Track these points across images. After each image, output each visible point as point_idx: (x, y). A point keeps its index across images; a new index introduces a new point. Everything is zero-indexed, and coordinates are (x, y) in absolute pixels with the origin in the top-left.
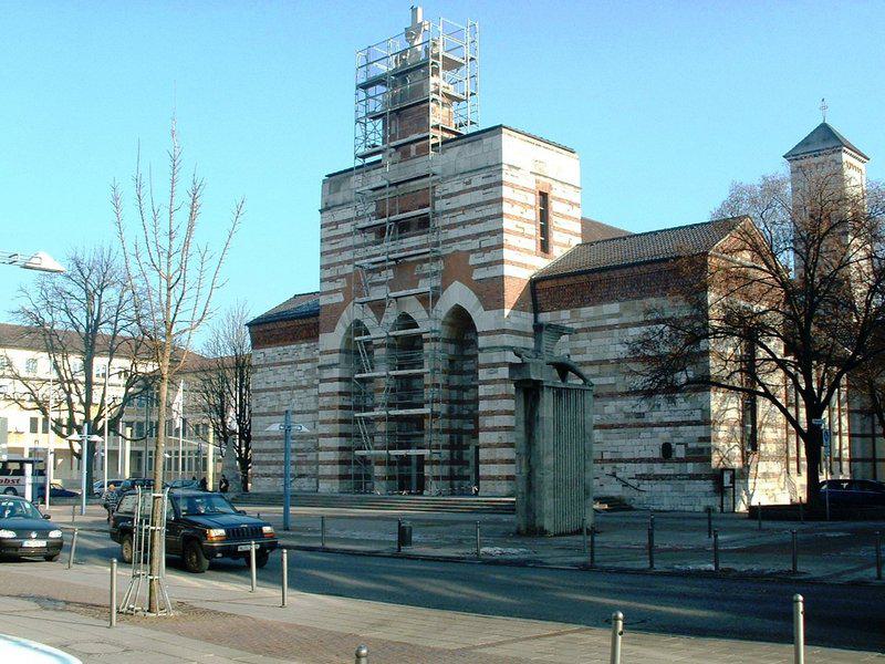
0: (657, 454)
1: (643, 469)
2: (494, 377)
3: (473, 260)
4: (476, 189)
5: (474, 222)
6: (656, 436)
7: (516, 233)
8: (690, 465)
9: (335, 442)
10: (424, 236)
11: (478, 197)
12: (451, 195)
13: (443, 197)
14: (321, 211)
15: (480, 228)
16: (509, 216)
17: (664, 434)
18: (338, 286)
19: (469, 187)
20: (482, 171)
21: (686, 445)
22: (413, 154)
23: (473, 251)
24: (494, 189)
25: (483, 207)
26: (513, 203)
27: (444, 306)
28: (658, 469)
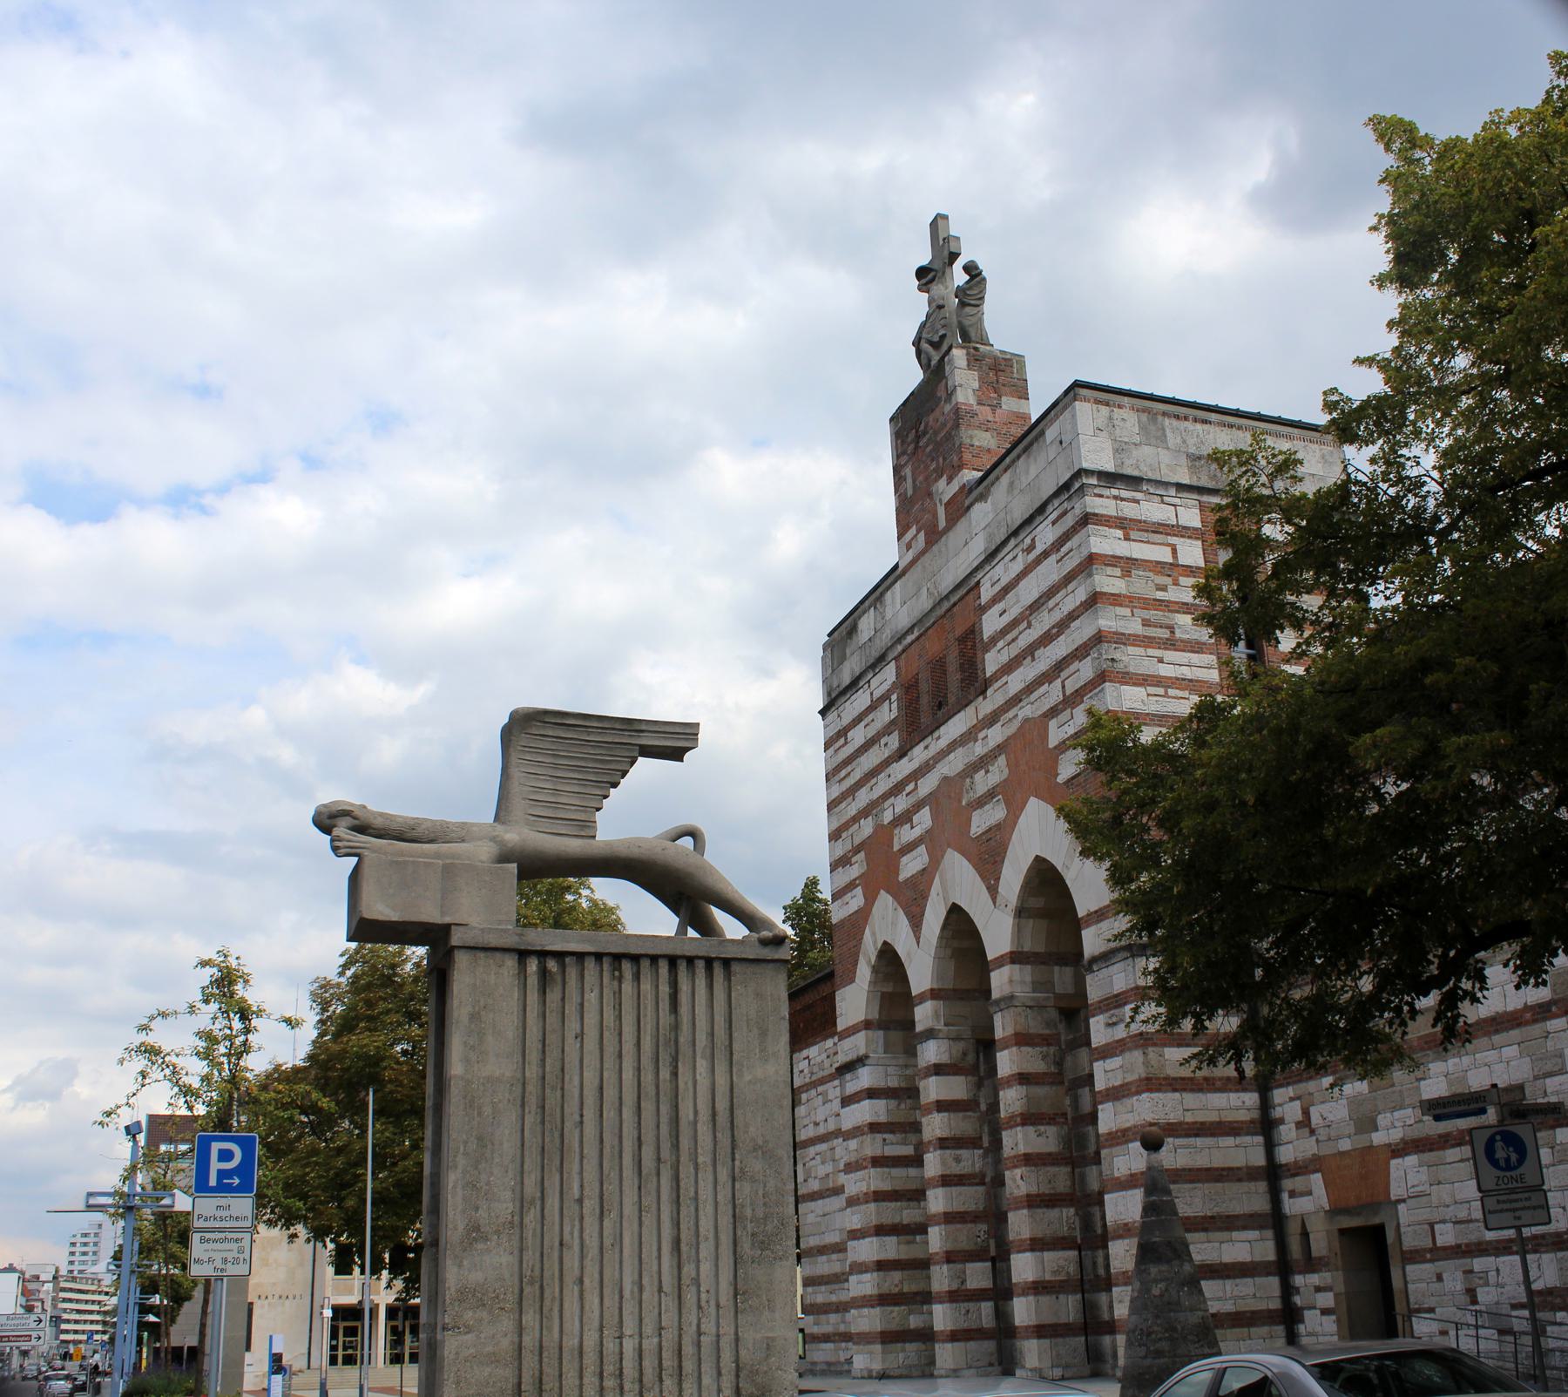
4: (1045, 554)
5: (1047, 639)
7: (1147, 642)
9: (867, 1250)
10: (970, 710)
11: (1050, 572)
12: (1006, 590)
13: (995, 600)
14: (823, 712)
15: (1060, 649)
16: (1116, 600)
18: (854, 871)
19: (1032, 556)
22: (942, 523)
23: (1053, 712)
26: (1128, 565)
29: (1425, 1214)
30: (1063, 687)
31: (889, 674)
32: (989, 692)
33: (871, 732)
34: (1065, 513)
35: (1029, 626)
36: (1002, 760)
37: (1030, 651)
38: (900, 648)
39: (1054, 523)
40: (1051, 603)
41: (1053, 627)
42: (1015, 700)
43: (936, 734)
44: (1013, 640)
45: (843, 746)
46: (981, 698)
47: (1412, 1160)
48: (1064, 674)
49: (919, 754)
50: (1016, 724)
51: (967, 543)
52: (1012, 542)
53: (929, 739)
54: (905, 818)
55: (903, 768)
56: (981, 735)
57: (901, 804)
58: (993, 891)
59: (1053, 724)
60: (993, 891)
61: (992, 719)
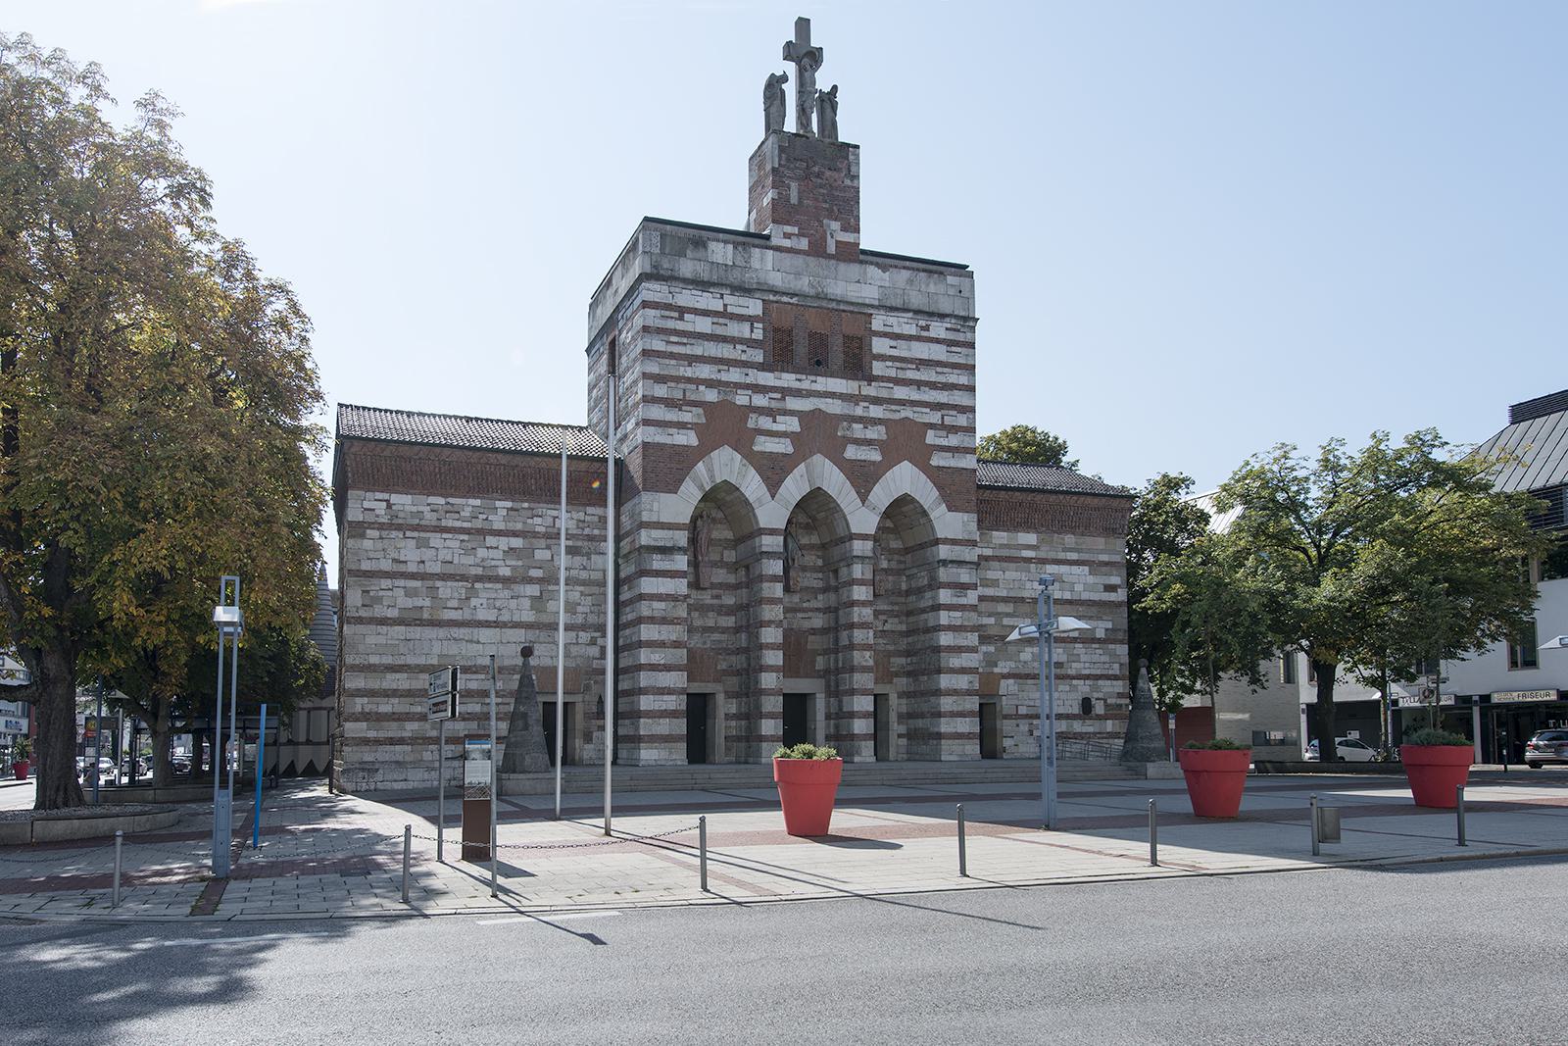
0: (1076, 710)
1: (1062, 726)
2: (963, 601)
3: (931, 438)
4: (937, 341)
5: (933, 386)
6: (1074, 688)
8: (1109, 722)
11: (939, 352)
17: (1083, 688)
18: (686, 417)
20: (948, 320)
21: (1105, 701)
23: (932, 426)
24: (964, 350)
25: (945, 370)
27: (883, 494)
28: (1078, 726)
29: (1017, 702)
30: (943, 418)
31: (754, 307)
32: (873, 384)
33: (720, 331)
34: (959, 331)
35: (919, 370)
36: (882, 429)
37: (919, 384)
40: (939, 369)
42: (902, 403)
43: (813, 378)
44: (902, 369)
45: (676, 319)
46: (866, 383)
47: (1011, 681)
48: (944, 412)
49: (788, 380)
50: (897, 416)
51: (858, 282)
52: (910, 315)
53: (804, 377)
55: (767, 379)
56: (863, 404)
57: (760, 401)
58: (864, 497)
59: (930, 433)
60: (864, 498)
61: (876, 401)
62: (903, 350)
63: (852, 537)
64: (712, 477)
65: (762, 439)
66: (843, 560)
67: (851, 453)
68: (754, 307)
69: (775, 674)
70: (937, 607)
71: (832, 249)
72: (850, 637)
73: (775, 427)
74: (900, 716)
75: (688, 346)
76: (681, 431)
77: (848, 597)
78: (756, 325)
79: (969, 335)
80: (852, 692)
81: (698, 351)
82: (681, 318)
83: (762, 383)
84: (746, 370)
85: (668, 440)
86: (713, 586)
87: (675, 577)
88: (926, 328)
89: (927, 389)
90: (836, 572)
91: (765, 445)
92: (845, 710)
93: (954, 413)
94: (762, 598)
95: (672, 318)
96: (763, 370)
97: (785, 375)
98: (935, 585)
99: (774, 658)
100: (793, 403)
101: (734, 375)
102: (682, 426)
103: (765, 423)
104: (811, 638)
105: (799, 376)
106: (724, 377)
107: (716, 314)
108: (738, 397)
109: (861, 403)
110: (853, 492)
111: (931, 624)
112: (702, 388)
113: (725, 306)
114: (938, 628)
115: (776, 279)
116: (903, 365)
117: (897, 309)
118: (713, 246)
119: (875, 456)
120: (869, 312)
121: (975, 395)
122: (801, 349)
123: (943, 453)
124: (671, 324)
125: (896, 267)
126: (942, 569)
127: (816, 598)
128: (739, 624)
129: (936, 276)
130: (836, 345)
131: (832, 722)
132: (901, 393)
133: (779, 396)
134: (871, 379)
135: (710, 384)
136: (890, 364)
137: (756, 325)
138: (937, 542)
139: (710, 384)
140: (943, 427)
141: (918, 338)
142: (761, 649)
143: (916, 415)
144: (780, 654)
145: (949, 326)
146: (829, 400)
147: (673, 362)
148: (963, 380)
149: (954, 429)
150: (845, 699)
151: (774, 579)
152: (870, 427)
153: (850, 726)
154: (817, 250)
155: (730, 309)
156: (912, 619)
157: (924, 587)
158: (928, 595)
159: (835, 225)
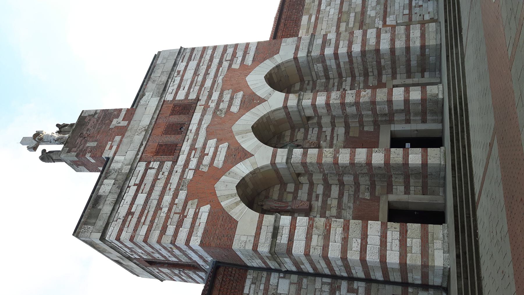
2: (333, 41)
3: (236, 66)
4: (186, 66)
5: (209, 67)
10: (198, 107)
11: (193, 64)
15: (216, 61)
18: (191, 212)
23: (230, 65)
24: (195, 53)
25: (202, 61)
30: (227, 61)
31: (142, 166)
32: (200, 98)
34: (184, 56)
35: (199, 74)
36: (226, 92)
37: (207, 73)
38: (140, 154)
39: (182, 62)
40: (201, 64)
41: (208, 64)
43: (189, 131)
44: (196, 83)
45: (132, 217)
46: (199, 102)
48: (224, 60)
49: (186, 147)
51: (146, 108)
52: (170, 80)
53: (187, 137)
54: (203, 155)
58: (262, 100)
59: (234, 66)
60: (262, 100)
62: (186, 84)
63: (285, 107)
64: (232, 196)
65: (216, 162)
66: (300, 112)
67: (235, 109)
68: (142, 166)
69: (373, 154)
70: (336, 55)
71: (125, 123)
72: (351, 105)
73: (211, 154)
74: (409, 77)
75: (150, 210)
76: (199, 217)
77: (323, 108)
78: (151, 166)
79: (188, 51)
80: (390, 102)
81: (155, 202)
82: (133, 214)
83: (183, 162)
84: (174, 172)
85: (203, 226)
86: (309, 199)
87: (295, 227)
88: (179, 72)
89: (210, 70)
90: (309, 118)
91: (219, 162)
92: (403, 108)
93: (225, 55)
94: (317, 163)
95: (131, 220)
96: (177, 161)
97: (183, 149)
98: (322, 58)
99: (361, 154)
100: (199, 145)
101: (175, 179)
102: (196, 215)
103: (207, 160)
104: (351, 134)
105: (186, 140)
106: (174, 186)
107: (137, 191)
108: (188, 178)
109: (209, 105)
110: (258, 107)
111: (347, 60)
112: (176, 201)
113: (135, 185)
114: (350, 54)
115: (131, 155)
116: (195, 82)
117: (165, 87)
118: (101, 192)
119: (240, 94)
120: (162, 102)
121: (219, 46)
122: (171, 139)
123: (246, 59)
124: (134, 220)
125: (145, 89)
126: (312, 54)
127: (325, 132)
128: (337, 182)
129: (155, 69)
130: (176, 119)
131: (411, 118)
132: (208, 83)
133: (194, 152)
134: (198, 99)
135: (175, 195)
136: (192, 90)
137: (151, 166)
138: (296, 58)
139: (175, 195)
140: (231, 61)
141: (183, 76)
142: (354, 164)
143: (222, 74)
144: (358, 150)
145: (181, 61)
146: (203, 123)
147: (156, 221)
148: (210, 52)
149: (234, 55)
150: (395, 107)
151: (305, 154)
152: (223, 99)
153: (415, 103)
154: (122, 131)
155: (137, 182)
156: (344, 74)
157: (323, 67)
158: (328, 63)
159: (115, 122)
